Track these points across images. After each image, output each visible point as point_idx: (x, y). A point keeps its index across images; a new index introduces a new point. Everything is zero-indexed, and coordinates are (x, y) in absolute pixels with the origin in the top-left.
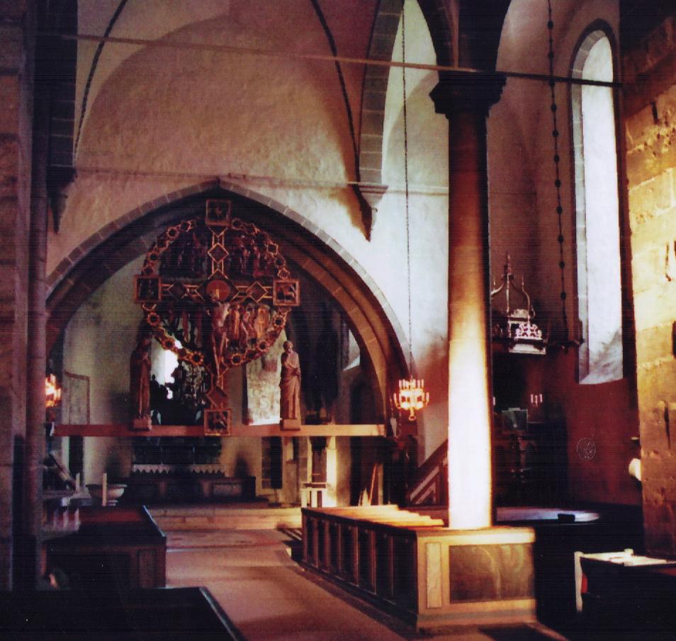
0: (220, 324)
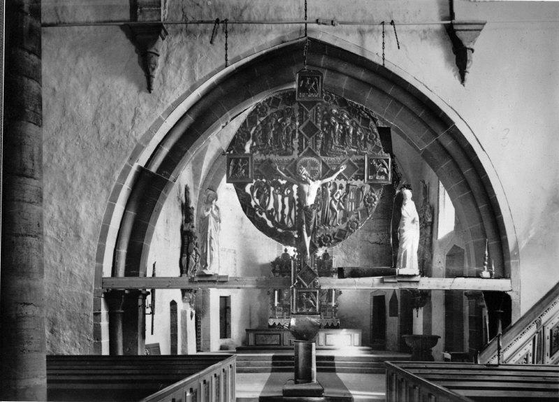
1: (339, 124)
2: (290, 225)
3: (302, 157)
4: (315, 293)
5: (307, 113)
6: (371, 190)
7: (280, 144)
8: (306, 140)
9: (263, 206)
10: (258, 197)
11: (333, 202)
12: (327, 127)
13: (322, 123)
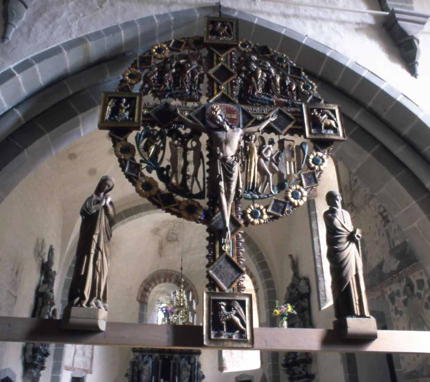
1: (263, 71)
2: (196, 190)
4: (242, 303)
5: (218, 56)
7: (183, 84)
9: (153, 163)
11: (262, 161)
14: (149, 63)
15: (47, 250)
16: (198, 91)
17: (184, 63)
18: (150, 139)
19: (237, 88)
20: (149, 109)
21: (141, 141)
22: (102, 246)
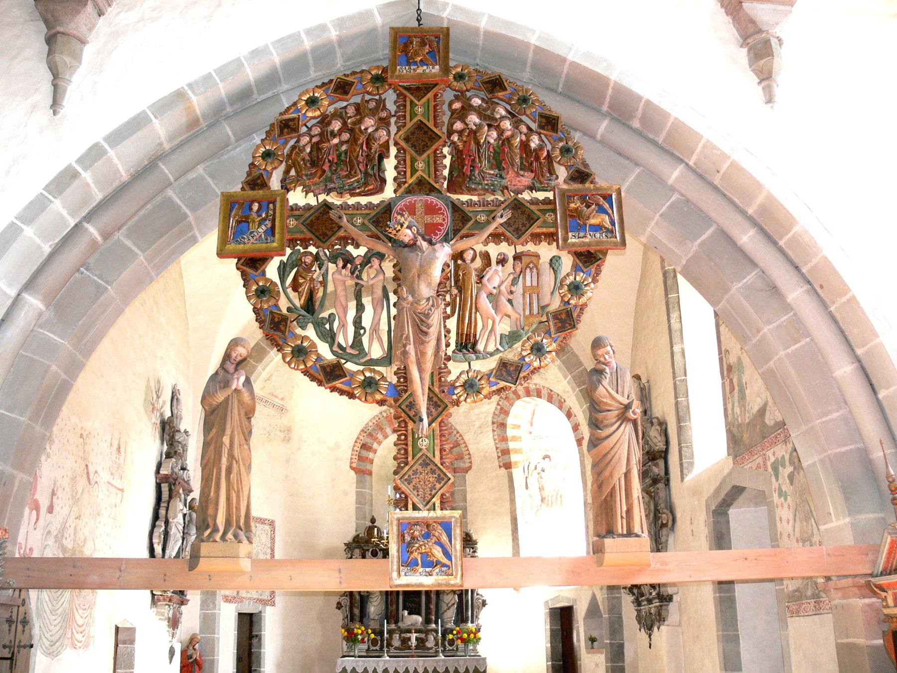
0: (426, 291)
1: (489, 126)
2: (376, 352)
3: (401, 198)
6: (576, 268)
8: (413, 161)
10: (295, 286)
12: (460, 133)
13: (451, 125)
14: (296, 130)
15: (167, 396)
16: (379, 175)
17: (354, 123)
18: (301, 270)
19: (447, 162)
20: (297, 218)
21: (286, 274)
22: (236, 453)
